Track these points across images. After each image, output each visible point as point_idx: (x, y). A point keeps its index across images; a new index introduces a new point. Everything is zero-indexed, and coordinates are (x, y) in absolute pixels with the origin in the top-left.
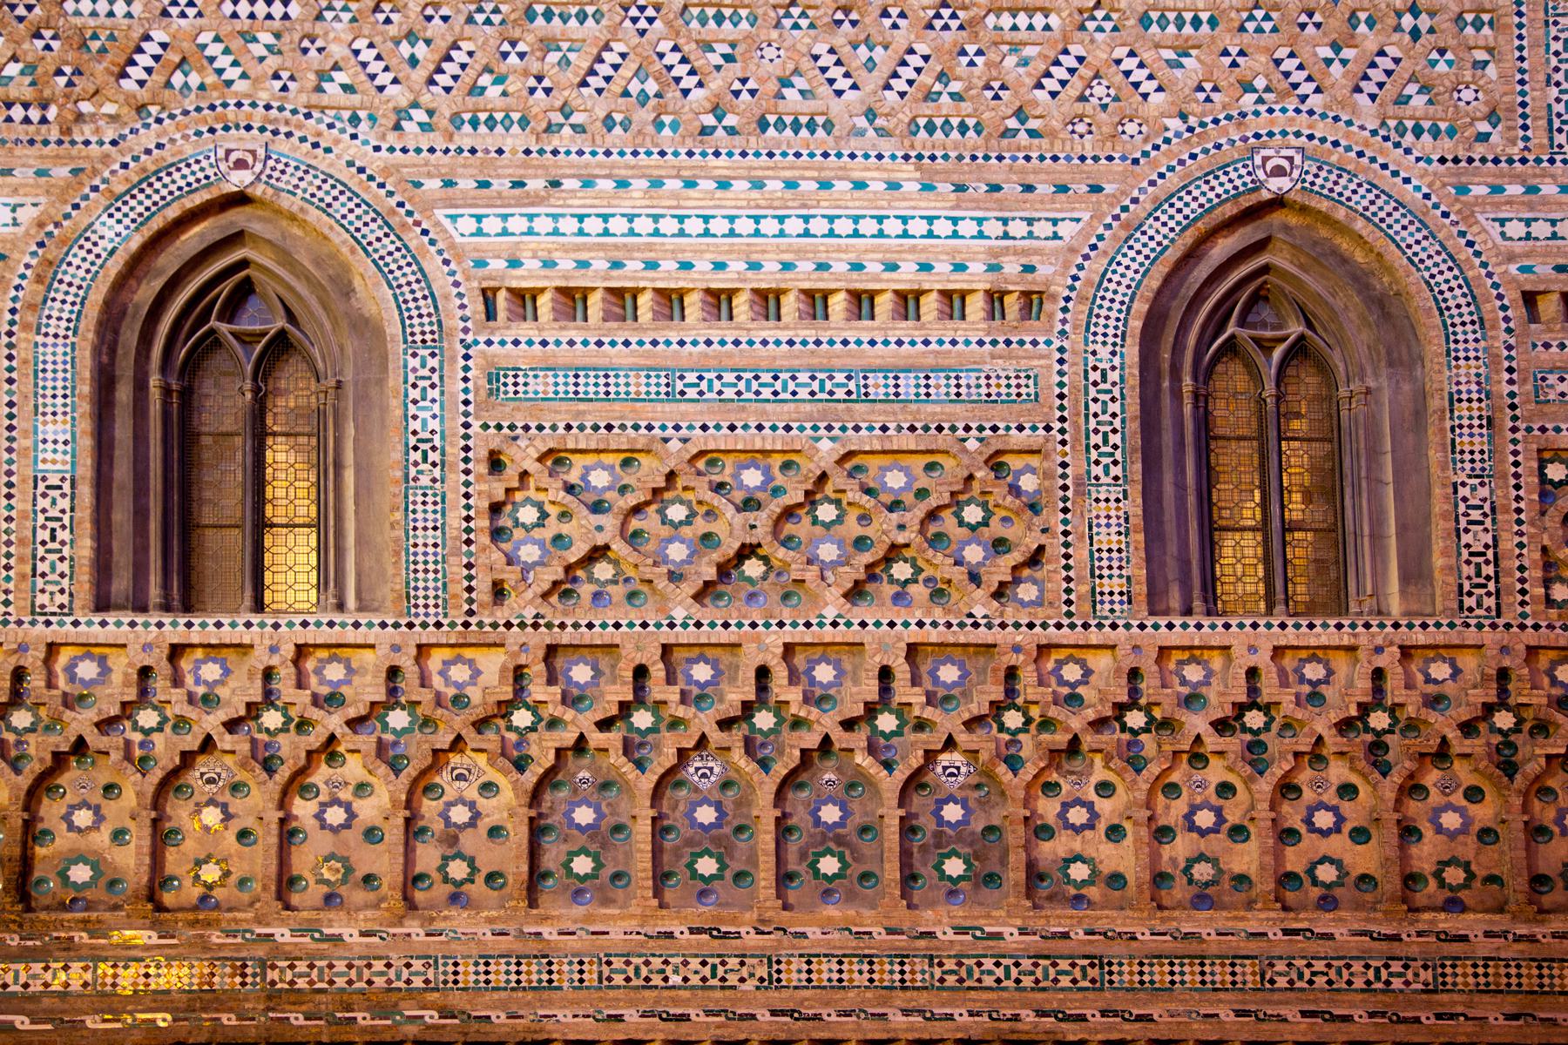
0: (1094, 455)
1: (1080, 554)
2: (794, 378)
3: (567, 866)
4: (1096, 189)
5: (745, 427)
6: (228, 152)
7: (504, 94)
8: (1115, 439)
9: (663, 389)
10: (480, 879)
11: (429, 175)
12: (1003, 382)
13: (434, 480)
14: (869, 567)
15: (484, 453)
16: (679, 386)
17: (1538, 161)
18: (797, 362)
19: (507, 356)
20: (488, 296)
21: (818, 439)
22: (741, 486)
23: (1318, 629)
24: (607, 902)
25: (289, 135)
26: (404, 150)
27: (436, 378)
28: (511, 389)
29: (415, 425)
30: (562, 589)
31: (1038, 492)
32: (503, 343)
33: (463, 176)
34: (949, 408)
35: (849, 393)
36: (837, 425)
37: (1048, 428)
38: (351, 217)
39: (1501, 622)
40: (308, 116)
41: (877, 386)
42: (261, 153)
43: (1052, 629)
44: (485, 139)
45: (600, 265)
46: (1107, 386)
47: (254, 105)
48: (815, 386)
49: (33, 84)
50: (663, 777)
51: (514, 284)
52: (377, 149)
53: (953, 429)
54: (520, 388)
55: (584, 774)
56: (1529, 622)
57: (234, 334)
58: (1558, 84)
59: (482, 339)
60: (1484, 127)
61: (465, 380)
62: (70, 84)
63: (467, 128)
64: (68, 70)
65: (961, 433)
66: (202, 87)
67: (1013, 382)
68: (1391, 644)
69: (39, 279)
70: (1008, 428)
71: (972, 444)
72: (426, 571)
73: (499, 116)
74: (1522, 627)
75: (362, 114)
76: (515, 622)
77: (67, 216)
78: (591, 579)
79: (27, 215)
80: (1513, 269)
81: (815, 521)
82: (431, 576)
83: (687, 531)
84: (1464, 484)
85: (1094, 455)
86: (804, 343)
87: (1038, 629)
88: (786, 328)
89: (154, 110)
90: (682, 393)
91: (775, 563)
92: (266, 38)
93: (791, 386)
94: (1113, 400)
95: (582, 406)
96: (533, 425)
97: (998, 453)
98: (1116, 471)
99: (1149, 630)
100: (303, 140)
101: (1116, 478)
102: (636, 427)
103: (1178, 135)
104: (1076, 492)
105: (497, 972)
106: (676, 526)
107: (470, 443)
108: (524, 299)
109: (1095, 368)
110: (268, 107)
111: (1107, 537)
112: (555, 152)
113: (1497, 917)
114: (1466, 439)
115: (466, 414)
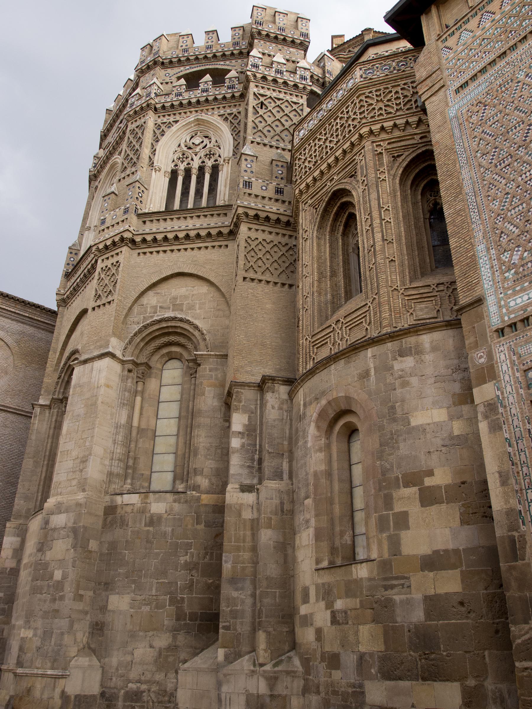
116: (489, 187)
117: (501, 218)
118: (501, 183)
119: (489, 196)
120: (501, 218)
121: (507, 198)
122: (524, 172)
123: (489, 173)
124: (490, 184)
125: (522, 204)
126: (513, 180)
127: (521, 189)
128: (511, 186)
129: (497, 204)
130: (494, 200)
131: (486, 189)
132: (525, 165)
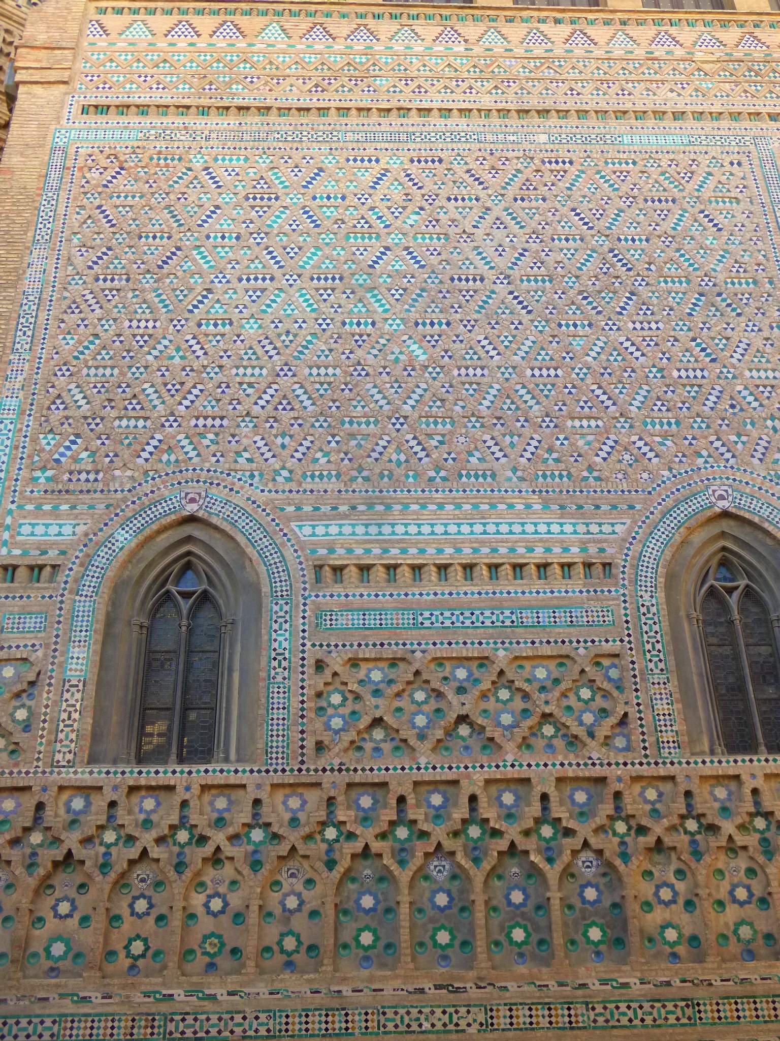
0: (648, 656)
1: (648, 716)
2: (482, 614)
3: (357, 939)
5: (457, 643)
6: (187, 494)
7: (329, 461)
8: (659, 646)
9: (411, 622)
10: (303, 949)
11: (289, 504)
12: (595, 614)
13: (284, 678)
14: (531, 728)
15: (313, 661)
16: (420, 619)
18: (483, 604)
19: (327, 604)
20: (319, 568)
21: (497, 650)
22: (455, 678)
24: (383, 966)
25: (218, 484)
26: (277, 492)
27: (288, 618)
28: (328, 622)
29: (275, 645)
30: (356, 746)
31: (620, 679)
32: (324, 596)
33: (306, 505)
34: (568, 630)
35: (513, 622)
36: (507, 641)
37: (622, 641)
38: (247, 527)
40: (228, 475)
41: (527, 617)
42: (203, 494)
43: (638, 766)
44: (318, 485)
45: (377, 551)
46: (650, 616)
47: (202, 470)
48: (494, 618)
49: (94, 461)
50: (415, 873)
51: (331, 562)
52: (263, 491)
53: (571, 642)
54: (334, 622)
55: (368, 872)
57: (179, 593)
59: (313, 594)
61: (304, 618)
62: (111, 461)
63: (309, 479)
64: (111, 454)
65: (575, 644)
66: (177, 461)
67: (601, 614)
69: (82, 565)
70: (600, 641)
71: (581, 651)
72: (278, 736)
73: (325, 473)
75: (256, 473)
76: (328, 768)
77: (101, 530)
78: (372, 740)
79: (80, 529)
81: (498, 700)
82: (280, 738)
83: (426, 708)
85: (648, 656)
86: (487, 593)
87: (629, 766)
88: (477, 585)
89: (151, 473)
90: (422, 623)
91: (476, 727)
92: (211, 436)
93: (481, 619)
94: (655, 623)
95: (367, 632)
96: (340, 644)
97: (597, 656)
98: (661, 665)
99: (692, 765)
100: (225, 487)
101: (662, 670)
102: (397, 644)
104: (642, 679)
105: (313, 1023)
106: (419, 704)
107: (305, 655)
108: (338, 570)
109: (643, 605)
110: (209, 471)
111: (662, 706)
112: (354, 491)
115: (304, 638)
116: (70, 308)
117: (68, 370)
118: (93, 311)
119: (63, 321)
120: (68, 370)
121: (92, 343)
122: (138, 317)
123: (81, 282)
124: (74, 302)
125: (113, 368)
126: (115, 320)
127: (121, 342)
128: (106, 327)
129: (71, 342)
130: (69, 333)
131: (64, 307)
132: (144, 306)
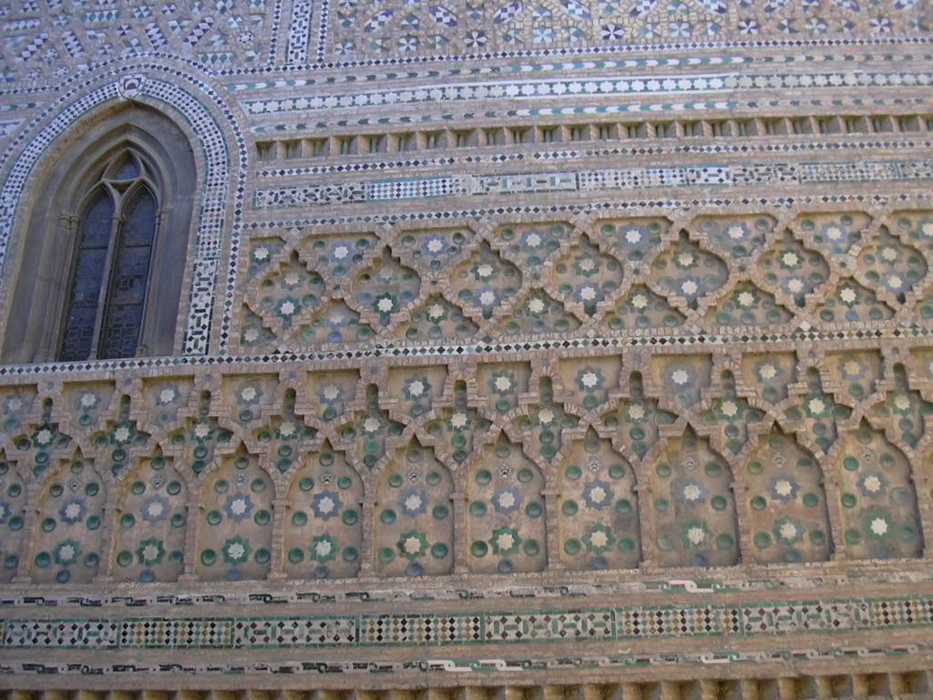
4: (31, 106)
17: (277, 69)
23: (92, 369)
39: (207, 358)
56: (225, 357)
58: (294, 29)
60: (251, 54)
68: (136, 377)
74: (220, 360)
80: (253, 129)
84: (201, 265)
103: (83, 72)
113: (169, 585)
114: (206, 235)
